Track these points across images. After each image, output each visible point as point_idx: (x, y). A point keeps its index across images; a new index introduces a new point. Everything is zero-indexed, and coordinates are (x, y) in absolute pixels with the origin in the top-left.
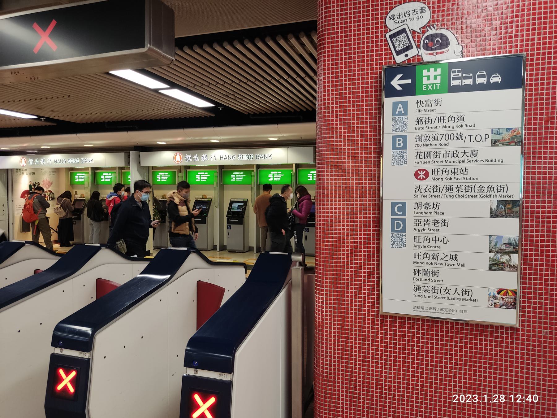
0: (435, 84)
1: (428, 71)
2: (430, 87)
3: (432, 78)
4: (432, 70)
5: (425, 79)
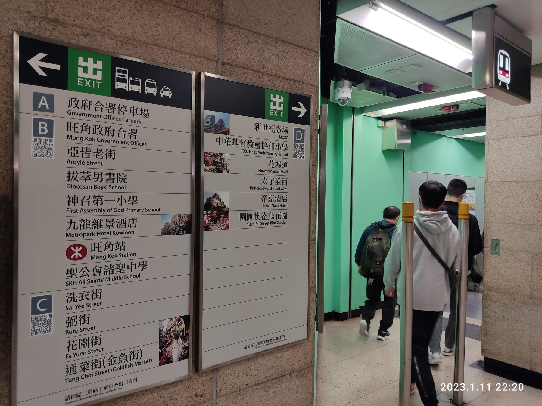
0: (95, 80)
1: (86, 60)
2: (88, 83)
3: (90, 71)
5: (81, 70)
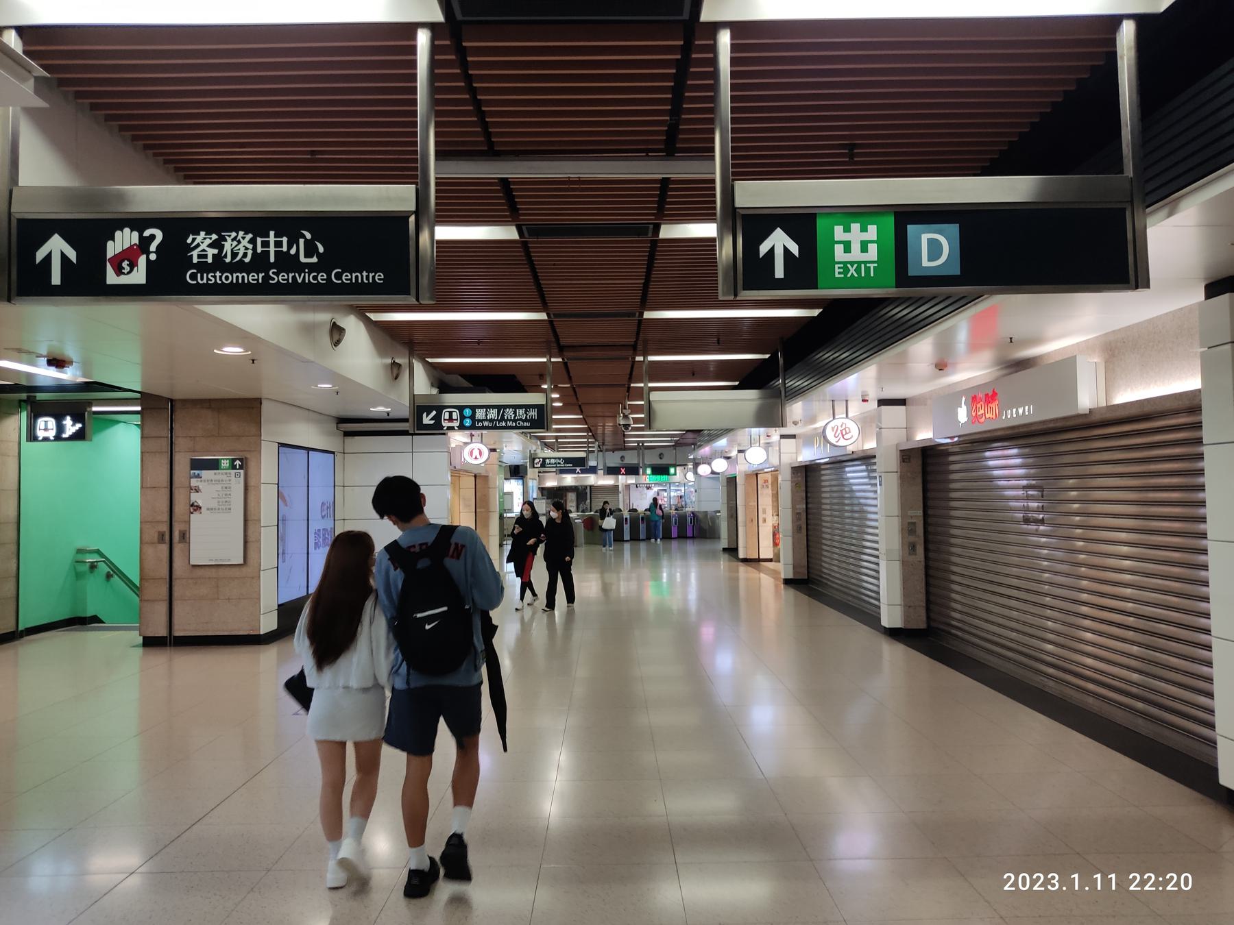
0: (865, 263)
1: (847, 230)
2: (852, 270)
3: (856, 247)
4: (855, 227)
5: (839, 249)
